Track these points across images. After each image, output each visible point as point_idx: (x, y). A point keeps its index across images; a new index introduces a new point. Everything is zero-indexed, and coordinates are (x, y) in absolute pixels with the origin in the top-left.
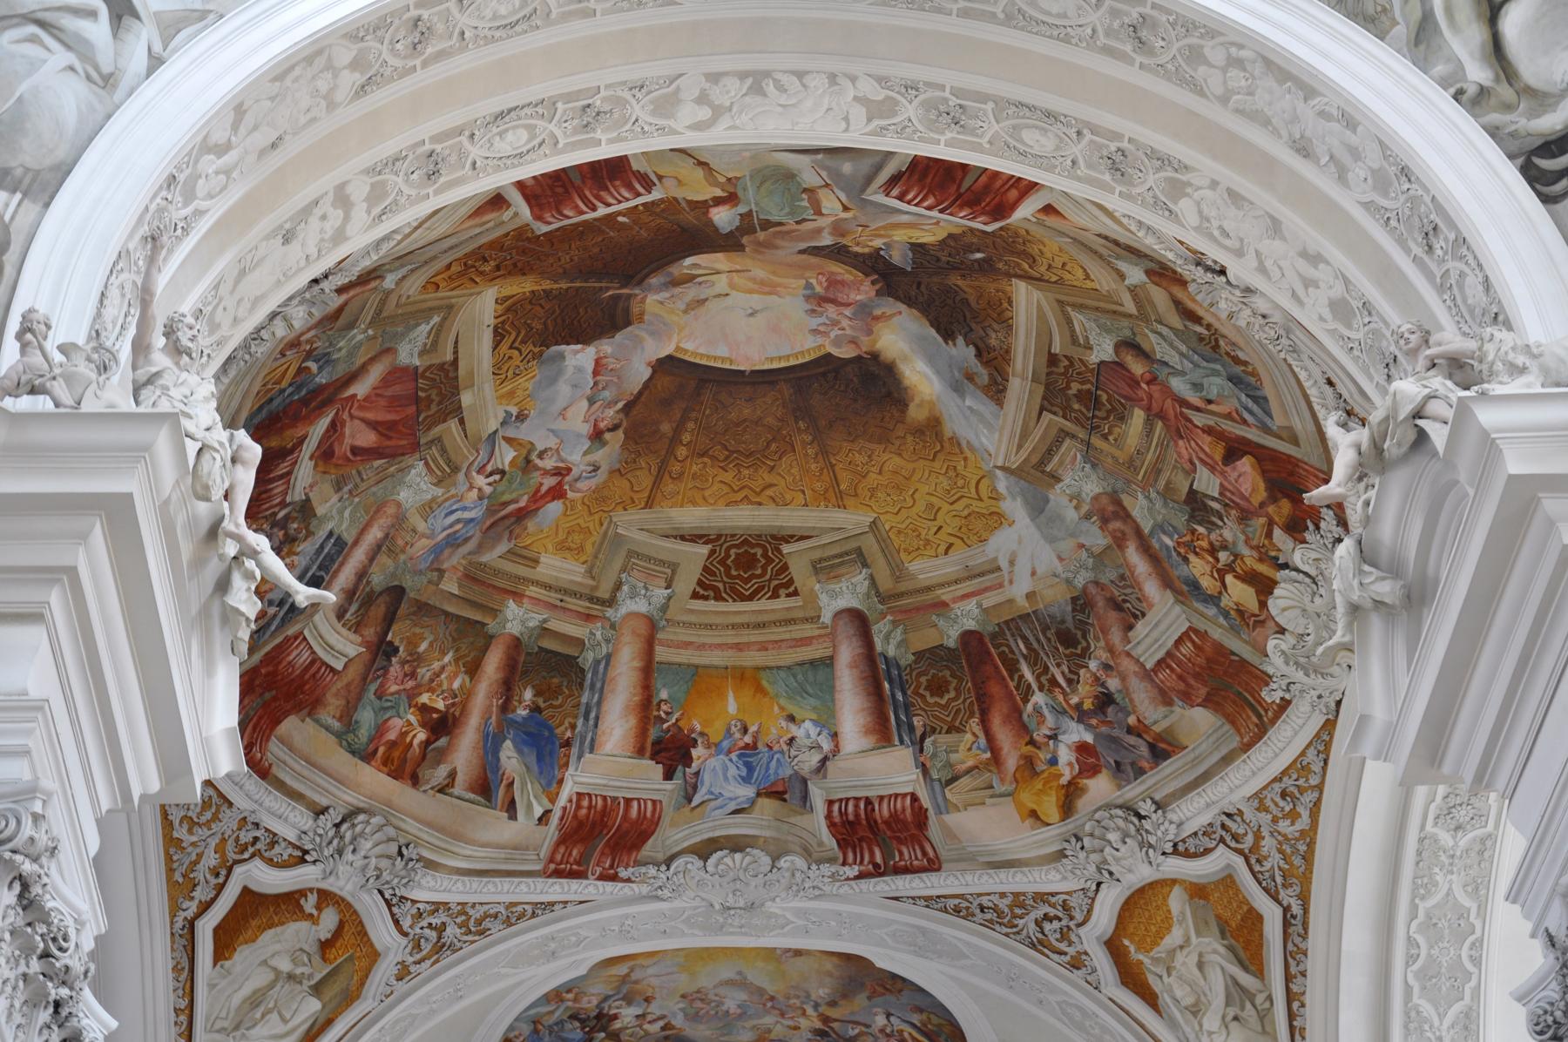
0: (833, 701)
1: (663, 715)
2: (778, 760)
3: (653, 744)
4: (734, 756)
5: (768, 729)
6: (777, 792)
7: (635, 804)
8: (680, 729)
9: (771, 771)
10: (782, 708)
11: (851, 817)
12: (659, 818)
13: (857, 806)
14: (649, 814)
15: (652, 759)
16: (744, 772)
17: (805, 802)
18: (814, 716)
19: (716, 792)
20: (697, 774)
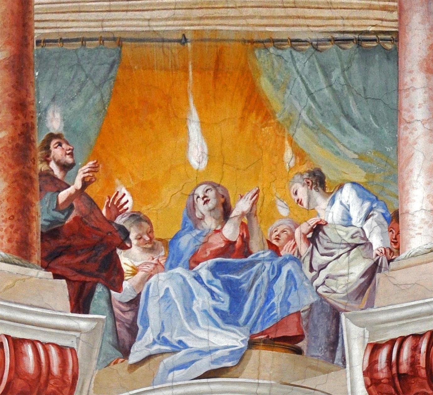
0: (396, 142)
1: (57, 172)
2: (290, 276)
3: (43, 235)
4: (203, 270)
5: (273, 205)
6: (285, 339)
7: (29, 350)
8: (93, 205)
9: (276, 300)
10: (299, 154)
11: (404, 368)
12: (75, 377)
13: (415, 349)
14: (55, 369)
15: (47, 268)
16: (225, 307)
17: (333, 352)
18: (360, 177)
19: (175, 338)
20: (134, 303)
